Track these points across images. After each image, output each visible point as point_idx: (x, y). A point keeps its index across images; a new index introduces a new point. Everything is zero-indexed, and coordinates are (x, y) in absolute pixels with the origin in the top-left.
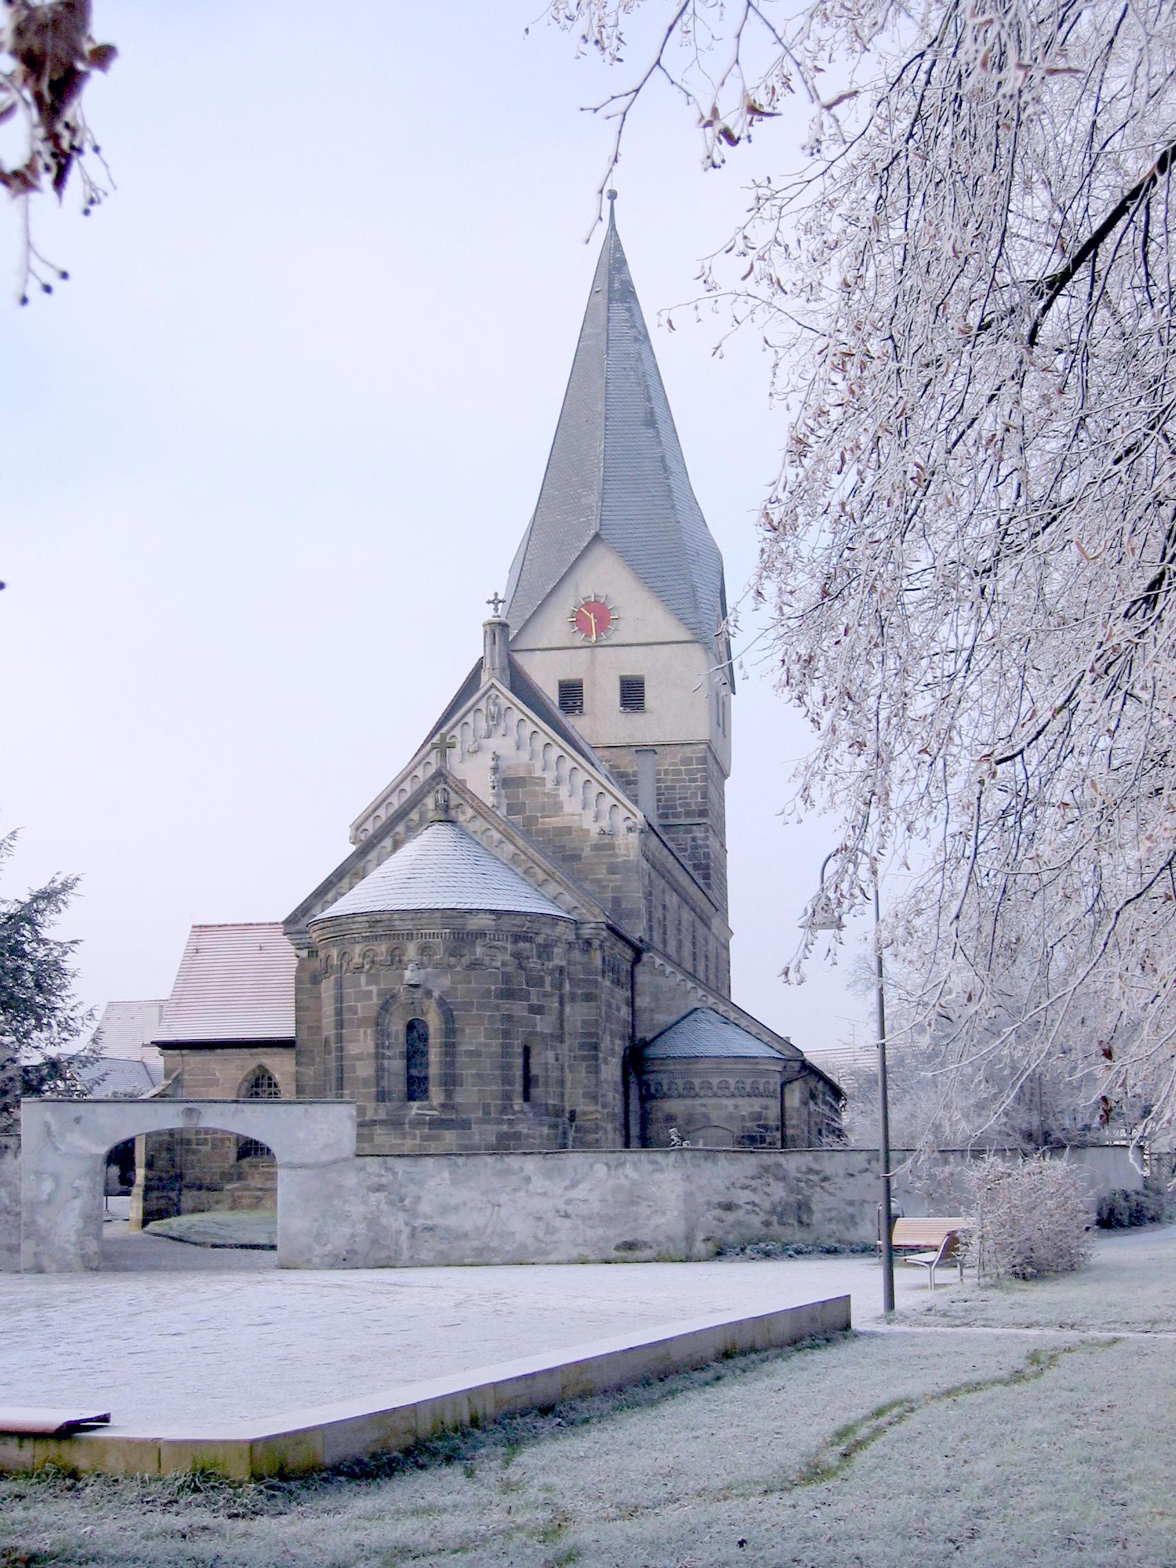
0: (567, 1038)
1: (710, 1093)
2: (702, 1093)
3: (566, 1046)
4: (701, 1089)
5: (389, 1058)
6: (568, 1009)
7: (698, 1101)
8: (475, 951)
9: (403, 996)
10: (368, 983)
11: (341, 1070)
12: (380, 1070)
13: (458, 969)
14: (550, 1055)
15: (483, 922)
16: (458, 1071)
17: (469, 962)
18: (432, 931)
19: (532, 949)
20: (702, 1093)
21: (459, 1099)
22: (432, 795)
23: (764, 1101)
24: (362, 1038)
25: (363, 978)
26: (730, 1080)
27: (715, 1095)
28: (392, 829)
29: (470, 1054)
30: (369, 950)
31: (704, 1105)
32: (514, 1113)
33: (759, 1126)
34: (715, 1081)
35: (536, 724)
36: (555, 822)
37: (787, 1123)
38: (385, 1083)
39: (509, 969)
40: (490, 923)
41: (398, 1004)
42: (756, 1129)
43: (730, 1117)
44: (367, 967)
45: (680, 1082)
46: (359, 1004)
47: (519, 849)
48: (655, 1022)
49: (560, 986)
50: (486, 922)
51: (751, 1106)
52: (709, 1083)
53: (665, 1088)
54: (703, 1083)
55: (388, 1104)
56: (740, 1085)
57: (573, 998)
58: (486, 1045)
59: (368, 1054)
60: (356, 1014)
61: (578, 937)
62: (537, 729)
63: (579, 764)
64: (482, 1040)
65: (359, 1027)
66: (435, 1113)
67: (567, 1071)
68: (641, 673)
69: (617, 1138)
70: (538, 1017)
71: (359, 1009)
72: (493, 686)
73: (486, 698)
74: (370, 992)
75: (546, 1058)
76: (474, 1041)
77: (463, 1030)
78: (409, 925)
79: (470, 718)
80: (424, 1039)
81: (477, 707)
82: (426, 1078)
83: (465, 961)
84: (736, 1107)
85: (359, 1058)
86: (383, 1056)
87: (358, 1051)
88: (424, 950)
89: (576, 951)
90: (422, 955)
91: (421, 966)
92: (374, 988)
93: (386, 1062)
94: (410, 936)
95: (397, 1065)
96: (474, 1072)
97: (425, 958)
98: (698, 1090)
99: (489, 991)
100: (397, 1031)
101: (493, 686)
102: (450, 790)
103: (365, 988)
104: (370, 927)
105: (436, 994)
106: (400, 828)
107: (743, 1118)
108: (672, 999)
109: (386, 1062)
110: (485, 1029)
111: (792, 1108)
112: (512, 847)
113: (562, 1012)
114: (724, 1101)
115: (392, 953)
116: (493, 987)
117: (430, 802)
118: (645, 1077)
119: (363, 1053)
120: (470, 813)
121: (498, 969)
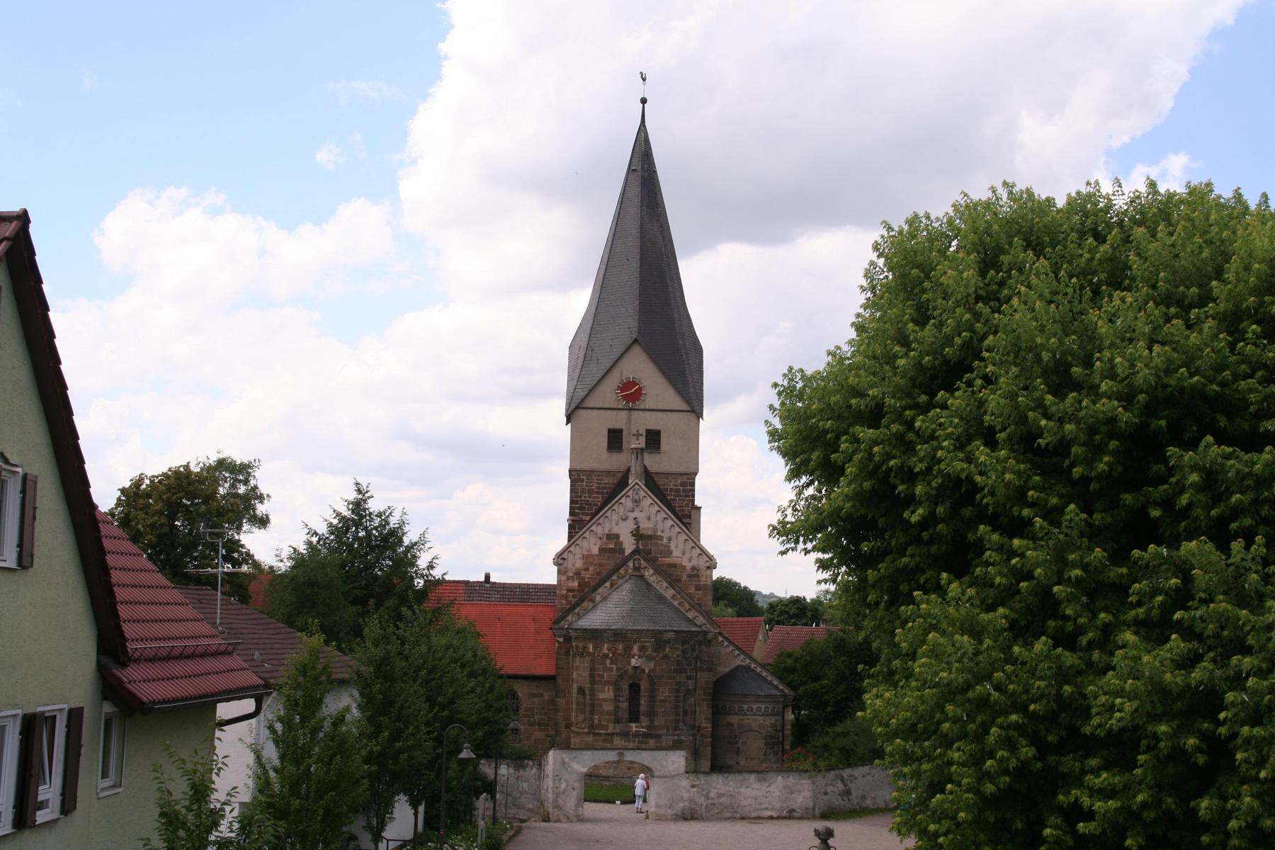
5: (622, 702)
7: (745, 717)
10: (611, 663)
11: (593, 705)
12: (617, 707)
21: (656, 723)
22: (632, 561)
23: (776, 718)
25: (608, 661)
27: (754, 715)
29: (661, 701)
32: (680, 730)
35: (659, 506)
36: (668, 560)
39: (680, 658)
44: (610, 655)
45: (736, 706)
50: (672, 635)
57: (701, 669)
59: (610, 700)
61: (705, 638)
64: (667, 694)
65: (605, 685)
66: (645, 730)
68: (659, 428)
72: (637, 483)
77: (658, 690)
78: (635, 636)
79: (623, 500)
83: (660, 655)
84: (764, 720)
86: (619, 701)
88: (642, 649)
92: (614, 666)
93: (620, 704)
94: (635, 642)
95: (625, 705)
101: (637, 483)
103: (608, 665)
105: (647, 671)
106: (614, 577)
109: (620, 704)
112: (672, 591)
114: (759, 718)
115: (625, 649)
117: (631, 564)
120: (651, 571)
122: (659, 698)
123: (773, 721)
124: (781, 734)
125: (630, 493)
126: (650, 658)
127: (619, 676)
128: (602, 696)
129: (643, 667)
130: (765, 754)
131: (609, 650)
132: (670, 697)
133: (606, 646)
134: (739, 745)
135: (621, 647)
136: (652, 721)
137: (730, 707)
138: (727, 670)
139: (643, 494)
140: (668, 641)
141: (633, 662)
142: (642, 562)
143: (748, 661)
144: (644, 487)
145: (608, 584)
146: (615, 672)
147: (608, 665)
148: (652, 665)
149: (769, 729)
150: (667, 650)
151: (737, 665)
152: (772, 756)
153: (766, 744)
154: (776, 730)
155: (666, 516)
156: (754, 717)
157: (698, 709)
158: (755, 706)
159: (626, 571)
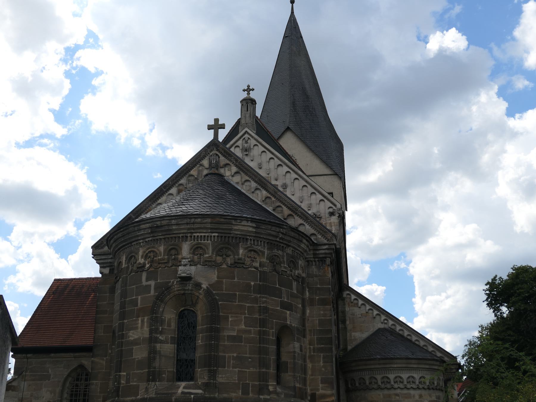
0: (308, 332)
1: (401, 386)
2: (396, 386)
3: (307, 340)
4: (395, 382)
5: (161, 342)
6: (308, 311)
7: (392, 392)
8: (239, 252)
9: (176, 287)
10: (147, 279)
12: (153, 353)
13: (224, 266)
14: (297, 345)
15: (245, 228)
16: (221, 354)
17: (233, 261)
18: (203, 234)
19: (283, 256)
20: (396, 386)
21: (221, 379)
22: (207, 158)
24: (139, 325)
25: (144, 275)
26: (415, 375)
27: (406, 388)
28: (178, 181)
30: (150, 252)
31: (397, 395)
32: (270, 393)
35: (273, 153)
38: (157, 364)
40: (251, 229)
41: (172, 295)
44: (147, 266)
45: (379, 377)
46: (139, 297)
47: (270, 193)
48: (353, 338)
49: (303, 293)
51: (430, 396)
52: (401, 377)
53: (367, 382)
54: (396, 377)
55: (157, 383)
57: (312, 302)
58: (245, 331)
60: (137, 306)
62: (273, 156)
63: (300, 176)
65: (138, 316)
66: (200, 391)
67: (308, 361)
70: (288, 312)
71: (139, 301)
73: (242, 139)
74: (150, 286)
75: (294, 348)
76: (236, 327)
77: (227, 318)
80: (193, 326)
81: (236, 145)
82: (193, 361)
83: (229, 261)
84: (421, 396)
85: (136, 342)
86: (157, 341)
87: (136, 337)
88: (196, 249)
89: (314, 267)
90: (194, 253)
91: (192, 263)
92: (152, 283)
93: (158, 346)
96: (235, 355)
97: (196, 257)
98: (392, 383)
99: (249, 285)
100: (170, 320)
102: (220, 155)
103: (144, 283)
104: (152, 232)
105: (204, 286)
109: (158, 346)
110: (245, 317)
112: (264, 193)
113: (304, 313)
114: (412, 392)
115: (168, 252)
116: (252, 283)
117: (205, 162)
119: (139, 338)
120: (234, 169)
121: (256, 268)
122: (226, 333)
125: (240, 143)
126: (209, 264)
127: (157, 298)
128: (133, 335)
129: (200, 280)
131: (146, 257)
132: (249, 332)
133: (141, 253)
135: (162, 249)
136: (213, 374)
137: (371, 378)
138: (365, 335)
139: (253, 142)
140: (243, 238)
141: (182, 271)
142: (222, 158)
143: (391, 322)
144: (253, 135)
145: (174, 190)
146: (152, 292)
147: (144, 283)
148: (213, 276)
150: (241, 251)
151: (376, 328)
155: (280, 163)
156: (405, 391)
157: (309, 365)
158: (405, 376)
159: (199, 172)
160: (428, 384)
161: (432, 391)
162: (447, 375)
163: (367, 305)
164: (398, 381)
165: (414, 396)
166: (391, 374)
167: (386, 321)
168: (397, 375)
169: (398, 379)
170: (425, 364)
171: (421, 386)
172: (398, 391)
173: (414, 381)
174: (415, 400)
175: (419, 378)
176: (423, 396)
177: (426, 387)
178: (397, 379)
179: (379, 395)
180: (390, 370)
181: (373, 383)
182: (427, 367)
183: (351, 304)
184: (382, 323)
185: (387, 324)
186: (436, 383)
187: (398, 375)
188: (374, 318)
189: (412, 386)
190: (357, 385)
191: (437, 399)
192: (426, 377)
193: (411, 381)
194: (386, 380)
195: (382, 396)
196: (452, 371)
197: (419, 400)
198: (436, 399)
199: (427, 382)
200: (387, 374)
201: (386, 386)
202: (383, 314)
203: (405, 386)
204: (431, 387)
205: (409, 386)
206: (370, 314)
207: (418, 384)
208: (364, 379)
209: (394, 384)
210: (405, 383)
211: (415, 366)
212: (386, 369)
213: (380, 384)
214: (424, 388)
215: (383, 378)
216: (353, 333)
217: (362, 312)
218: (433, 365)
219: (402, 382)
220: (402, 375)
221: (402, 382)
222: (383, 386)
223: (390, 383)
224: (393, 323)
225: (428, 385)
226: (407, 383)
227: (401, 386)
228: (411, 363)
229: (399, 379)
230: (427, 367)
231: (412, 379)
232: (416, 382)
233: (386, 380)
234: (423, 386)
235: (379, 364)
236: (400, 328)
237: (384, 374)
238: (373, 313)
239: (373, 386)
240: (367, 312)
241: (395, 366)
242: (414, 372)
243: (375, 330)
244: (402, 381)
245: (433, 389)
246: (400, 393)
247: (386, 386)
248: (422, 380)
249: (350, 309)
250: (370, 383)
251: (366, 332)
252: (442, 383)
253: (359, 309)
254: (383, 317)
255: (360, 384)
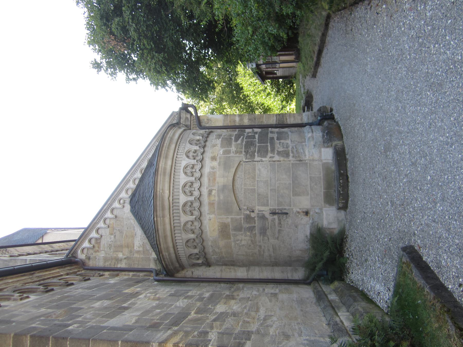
1: (196, 185)
2: (196, 193)
4: (192, 195)
7: (205, 199)
20: (196, 193)
31: (210, 192)
33: (236, 140)
34: (183, 179)
37: (237, 124)
42: (239, 141)
43: (226, 165)
45: (184, 218)
48: (141, 249)
51: (214, 146)
52: (185, 186)
53: (192, 236)
54: (185, 192)
56: (191, 154)
69: (242, 295)
84: (214, 158)
98: (192, 198)
107: (225, 152)
108: (121, 232)
111: (224, 121)
114: (207, 170)
118: (184, 260)
123: (219, 142)
124: (247, 130)
130: (286, 154)
134: (266, 210)
137: (185, 230)
138: (139, 232)
149: (233, 148)
151: (130, 215)
152: (289, 142)
153: (263, 152)
154: (236, 140)
156: (205, 180)
158: (183, 179)
160: (197, 148)
161: (208, 143)
162: (194, 126)
163: (99, 226)
164: (189, 189)
165: (213, 168)
166: (179, 199)
167: (122, 201)
168: (181, 191)
169: (187, 189)
170: (169, 148)
171: (200, 157)
172: (205, 191)
173: (191, 166)
174: (218, 166)
175: (187, 159)
176: (213, 155)
177: (202, 150)
178: (187, 191)
179: (210, 220)
180: (173, 200)
181: (193, 227)
182: (173, 146)
183: (97, 248)
184: (124, 207)
185: (125, 200)
186: (198, 138)
187: (181, 188)
188: (116, 217)
189: (197, 170)
190: (196, 251)
191: (220, 138)
192: (187, 149)
193: (190, 170)
194: (188, 208)
195: (212, 216)
196: (189, 119)
197: (218, 161)
198: (220, 139)
199: (195, 149)
200: (179, 206)
201: (197, 209)
202: (111, 204)
203: (197, 179)
204: (203, 144)
205: (198, 175)
206: (111, 223)
207: (196, 161)
208: (188, 241)
209: (194, 197)
210: (192, 179)
211: (169, 163)
212: (171, 206)
213: (194, 217)
214: (202, 154)
215: (184, 212)
216: (135, 248)
217: (108, 234)
218: (171, 139)
219: (192, 183)
220: (182, 183)
221: (192, 183)
222: (196, 213)
223: (192, 203)
224: (124, 192)
225: (199, 147)
226: (192, 176)
227: (196, 185)
228: (165, 169)
229: (187, 187)
230: (173, 146)
231: (188, 168)
232: (193, 163)
233: (188, 208)
234: (200, 154)
235: (163, 217)
236: (131, 182)
237: (179, 209)
238: (110, 219)
239: (198, 228)
240: (108, 227)
241: (167, 192)
242: (179, 165)
243: (133, 217)
244: (190, 184)
245: (206, 141)
246: (207, 188)
247: (197, 209)
248: (191, 154)
249: (102, 251)
250: (193, 233)
251: (134, 230)
252: (202, 131)
253: (103, 237)
254: (116, 205)
255: (195, 247)
